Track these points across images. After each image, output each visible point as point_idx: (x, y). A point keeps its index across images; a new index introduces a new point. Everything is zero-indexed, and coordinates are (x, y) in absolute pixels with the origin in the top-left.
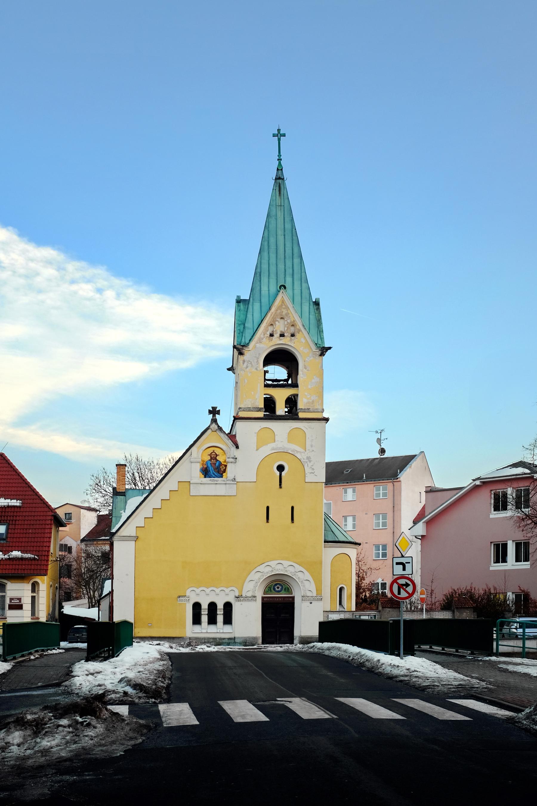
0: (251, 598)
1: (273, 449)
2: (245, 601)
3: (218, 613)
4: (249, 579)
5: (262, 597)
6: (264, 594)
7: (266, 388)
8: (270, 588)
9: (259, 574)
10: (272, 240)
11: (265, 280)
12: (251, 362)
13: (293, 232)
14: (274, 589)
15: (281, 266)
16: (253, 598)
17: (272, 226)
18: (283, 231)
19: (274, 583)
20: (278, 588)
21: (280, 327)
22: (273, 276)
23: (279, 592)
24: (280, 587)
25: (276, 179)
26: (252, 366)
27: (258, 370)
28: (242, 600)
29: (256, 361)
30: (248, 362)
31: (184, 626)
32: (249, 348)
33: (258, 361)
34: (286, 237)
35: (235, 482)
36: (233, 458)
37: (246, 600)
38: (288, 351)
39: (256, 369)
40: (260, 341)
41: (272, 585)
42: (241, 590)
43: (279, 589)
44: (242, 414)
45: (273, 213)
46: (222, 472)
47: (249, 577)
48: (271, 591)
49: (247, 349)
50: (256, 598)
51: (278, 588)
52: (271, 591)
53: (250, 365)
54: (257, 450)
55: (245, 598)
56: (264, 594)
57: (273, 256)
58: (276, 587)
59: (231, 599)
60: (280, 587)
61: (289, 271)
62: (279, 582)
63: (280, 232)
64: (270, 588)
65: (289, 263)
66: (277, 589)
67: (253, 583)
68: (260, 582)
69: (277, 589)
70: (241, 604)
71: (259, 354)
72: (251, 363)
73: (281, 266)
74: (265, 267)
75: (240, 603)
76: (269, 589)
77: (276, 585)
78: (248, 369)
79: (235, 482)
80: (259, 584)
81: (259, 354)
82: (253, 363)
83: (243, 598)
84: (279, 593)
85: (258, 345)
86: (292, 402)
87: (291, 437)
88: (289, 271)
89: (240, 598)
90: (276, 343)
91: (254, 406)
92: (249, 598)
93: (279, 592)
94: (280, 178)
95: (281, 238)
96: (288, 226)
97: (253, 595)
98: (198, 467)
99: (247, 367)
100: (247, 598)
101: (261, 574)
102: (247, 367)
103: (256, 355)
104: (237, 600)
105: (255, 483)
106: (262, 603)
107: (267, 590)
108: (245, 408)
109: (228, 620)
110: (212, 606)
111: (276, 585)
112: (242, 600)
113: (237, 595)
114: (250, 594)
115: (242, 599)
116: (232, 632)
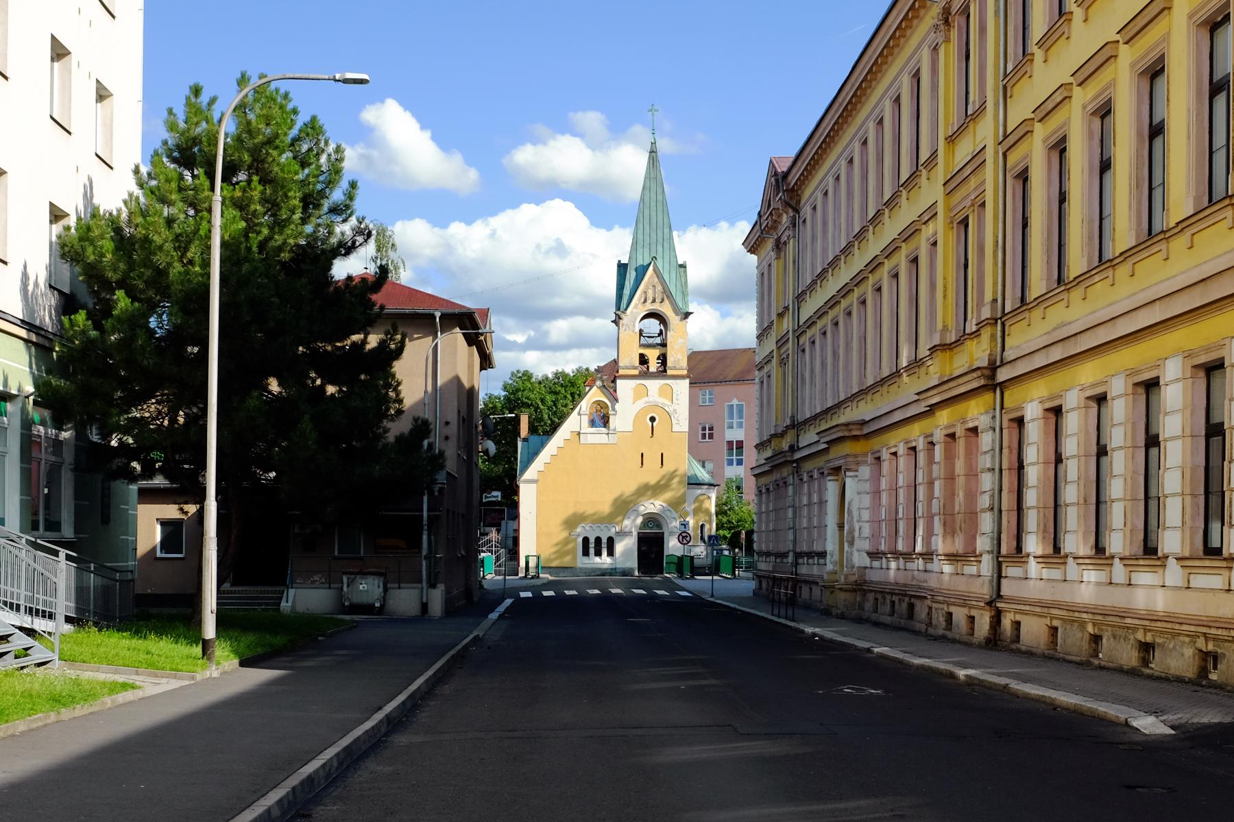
1: (646, 403)
10: (646, 212)
11: (640, 251)
17: (646, 199)
22: (647, 246)
25: (650, 152)
31: (575, 558)
33: (634, 325)
44: (621, 372)
45: (648, 185)
57: (647, 227)
61: (660, 240)
63: (653, 204)
74: (640, 237)
86: (663, 359)
87: (662, 392)
90: (650, 307)
94: (653, 152)
96: (660, 198)
98: (585, 419)
109: (611, 553)
110: (598, 540)
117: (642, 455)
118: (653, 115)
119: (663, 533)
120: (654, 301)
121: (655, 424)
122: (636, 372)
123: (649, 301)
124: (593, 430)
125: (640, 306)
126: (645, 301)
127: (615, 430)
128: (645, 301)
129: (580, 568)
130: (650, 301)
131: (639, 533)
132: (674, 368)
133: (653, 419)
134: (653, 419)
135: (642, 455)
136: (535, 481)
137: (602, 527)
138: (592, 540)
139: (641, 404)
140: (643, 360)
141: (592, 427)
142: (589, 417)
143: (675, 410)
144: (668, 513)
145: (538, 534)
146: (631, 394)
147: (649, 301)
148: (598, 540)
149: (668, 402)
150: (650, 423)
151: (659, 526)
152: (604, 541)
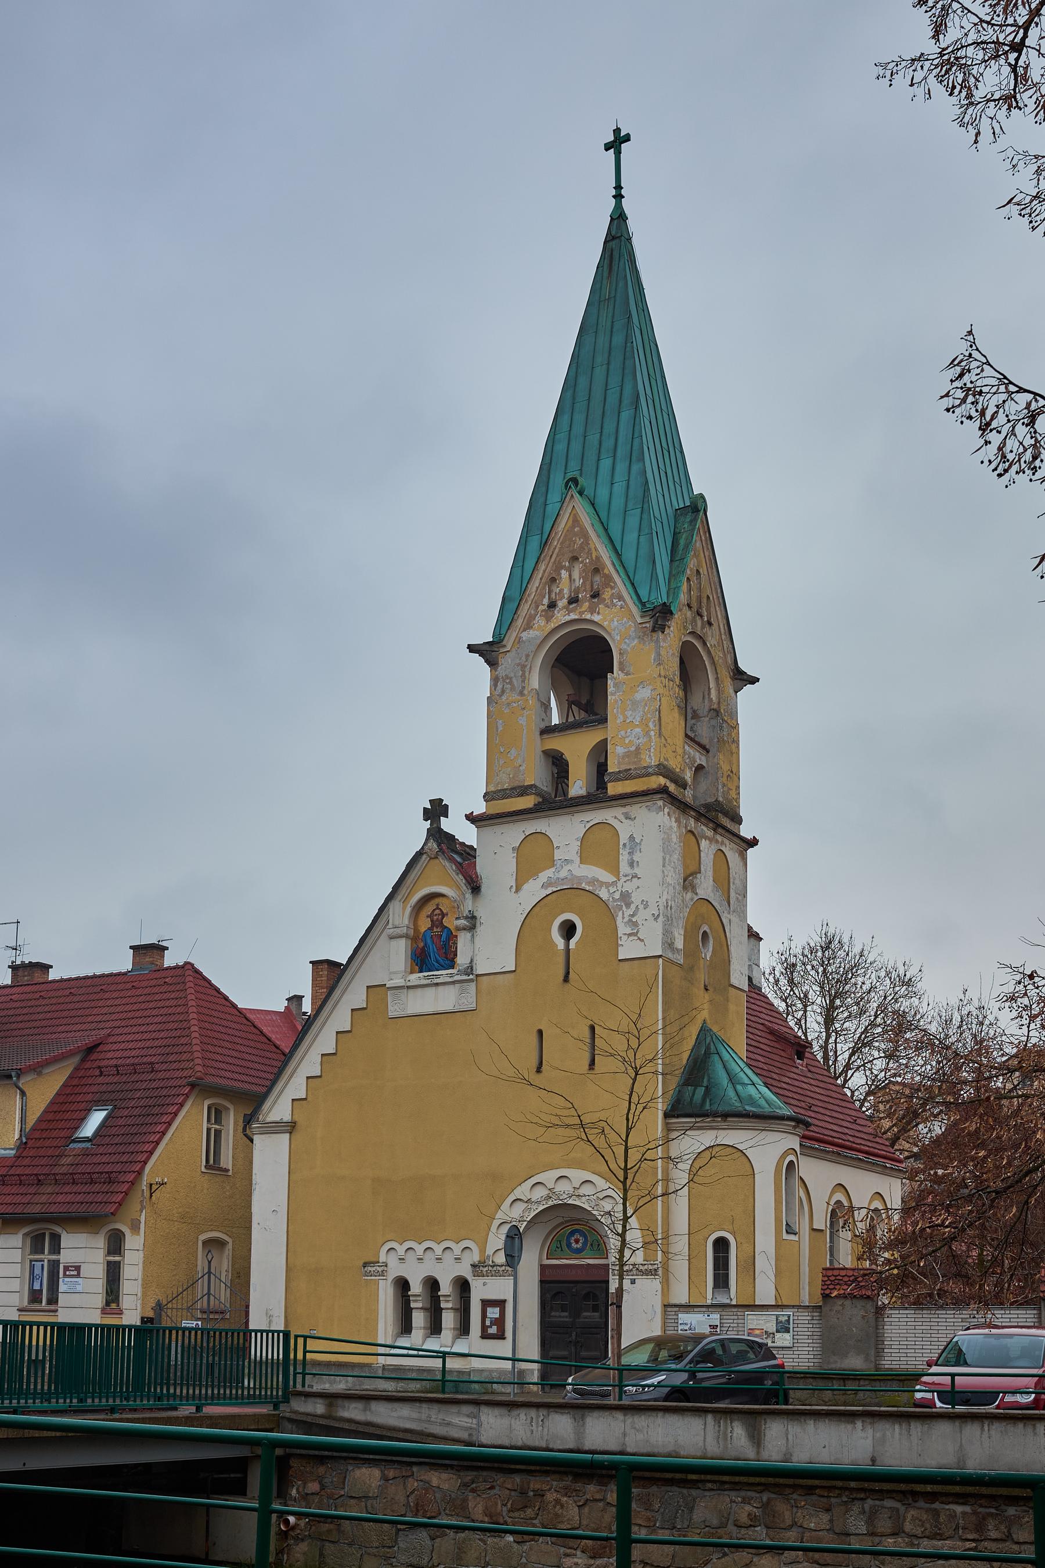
0: (503, 1268)
2: (492, 1276)
6: (547, 1259)
7: (545, 736)
9: (520, 1207)
10: (583, 382)
12: (511, 678)
13: (628, 349)
14: (569, 1245)
15: (593, 438)
18: (606, 355)
19: (569, 1230)
20: (577, 1241)
21: (567, 583)
23: (579, 1251)
26: (513, 689)
27: (524, 695)
28: (485, 1273)
29: (521, 672)
30: (504, 681)
32: (505, 646)
33: (523, 675)
34: (612, 367)
35: (471, 977)
36: (466, 918)
37: (493, 1273)
38: (581, 639)
39: (521, 693)
40: (528, 626)
43: (579, 1245)
46: (452, 956)
48: (562, 1250)
49: (502, 650)
51: (577, 1241)
52: (562, 1250)
53: (509, 686)
54: (517, 891)
55: (490, 1268)
56: (547, 1259)
57: (579, 418)
58: (572, 1241)
59: (466, 1272)
61: (608, 444)
62: (577, 1227)
65: (609, 427)
70: (484, 1284)
71: (527, 656)
72: (511, 683)
73: (593, 438)
74: (560, 447)
75: (481, 1281)
76: (559, 1246)
77: (572, 1233)
78: (504, 698)
79: (471, 977)
81: (527, 656)
82: (514, 680)
83: (486, 1269)
84: (578, 1256)
85: (525, 635)
88: (608, 444)
89: (481, 1268)
91: (516, 784)
93: (579, 1251)
95: (599, 373)
99: (503, 691)
100: (495, 1268)
101: (526, 1205)
102: (503, 691)
103: (520, 659)
104: (476, 1274)
105: (512, 975)
106: (542, 1282)
108: (494, 792)
113: (476, 1258)
117: (540, 1033)
118: (618, 154)
120: (573, 600)
121: (573, 942)
122: (527, 802)
123: (562, 603)
124: (415, 978)
125: (540, 621)
126: (552, 605)
127: (470, 970)
128: (552, 605)
130: (565, 601)
131: (543, 1268)
132: (626, 775)
133: (568, 930)
134: (568, 930)
135: (540, 1033)
136: (291, 1127)
137: (438, 1249)
138: (416, 1288)
139: (534, 890)
140: (558, 765)
141: (421, 971)
142: (414, 939)
143: (626, 897)
145: (288, 1270)
146: (508, 864)
147: (562, 603)
148: (432, 1285)
149: (605, 876)
150: (560, 943)
151: (599, 1247)
152: (446, 1288)
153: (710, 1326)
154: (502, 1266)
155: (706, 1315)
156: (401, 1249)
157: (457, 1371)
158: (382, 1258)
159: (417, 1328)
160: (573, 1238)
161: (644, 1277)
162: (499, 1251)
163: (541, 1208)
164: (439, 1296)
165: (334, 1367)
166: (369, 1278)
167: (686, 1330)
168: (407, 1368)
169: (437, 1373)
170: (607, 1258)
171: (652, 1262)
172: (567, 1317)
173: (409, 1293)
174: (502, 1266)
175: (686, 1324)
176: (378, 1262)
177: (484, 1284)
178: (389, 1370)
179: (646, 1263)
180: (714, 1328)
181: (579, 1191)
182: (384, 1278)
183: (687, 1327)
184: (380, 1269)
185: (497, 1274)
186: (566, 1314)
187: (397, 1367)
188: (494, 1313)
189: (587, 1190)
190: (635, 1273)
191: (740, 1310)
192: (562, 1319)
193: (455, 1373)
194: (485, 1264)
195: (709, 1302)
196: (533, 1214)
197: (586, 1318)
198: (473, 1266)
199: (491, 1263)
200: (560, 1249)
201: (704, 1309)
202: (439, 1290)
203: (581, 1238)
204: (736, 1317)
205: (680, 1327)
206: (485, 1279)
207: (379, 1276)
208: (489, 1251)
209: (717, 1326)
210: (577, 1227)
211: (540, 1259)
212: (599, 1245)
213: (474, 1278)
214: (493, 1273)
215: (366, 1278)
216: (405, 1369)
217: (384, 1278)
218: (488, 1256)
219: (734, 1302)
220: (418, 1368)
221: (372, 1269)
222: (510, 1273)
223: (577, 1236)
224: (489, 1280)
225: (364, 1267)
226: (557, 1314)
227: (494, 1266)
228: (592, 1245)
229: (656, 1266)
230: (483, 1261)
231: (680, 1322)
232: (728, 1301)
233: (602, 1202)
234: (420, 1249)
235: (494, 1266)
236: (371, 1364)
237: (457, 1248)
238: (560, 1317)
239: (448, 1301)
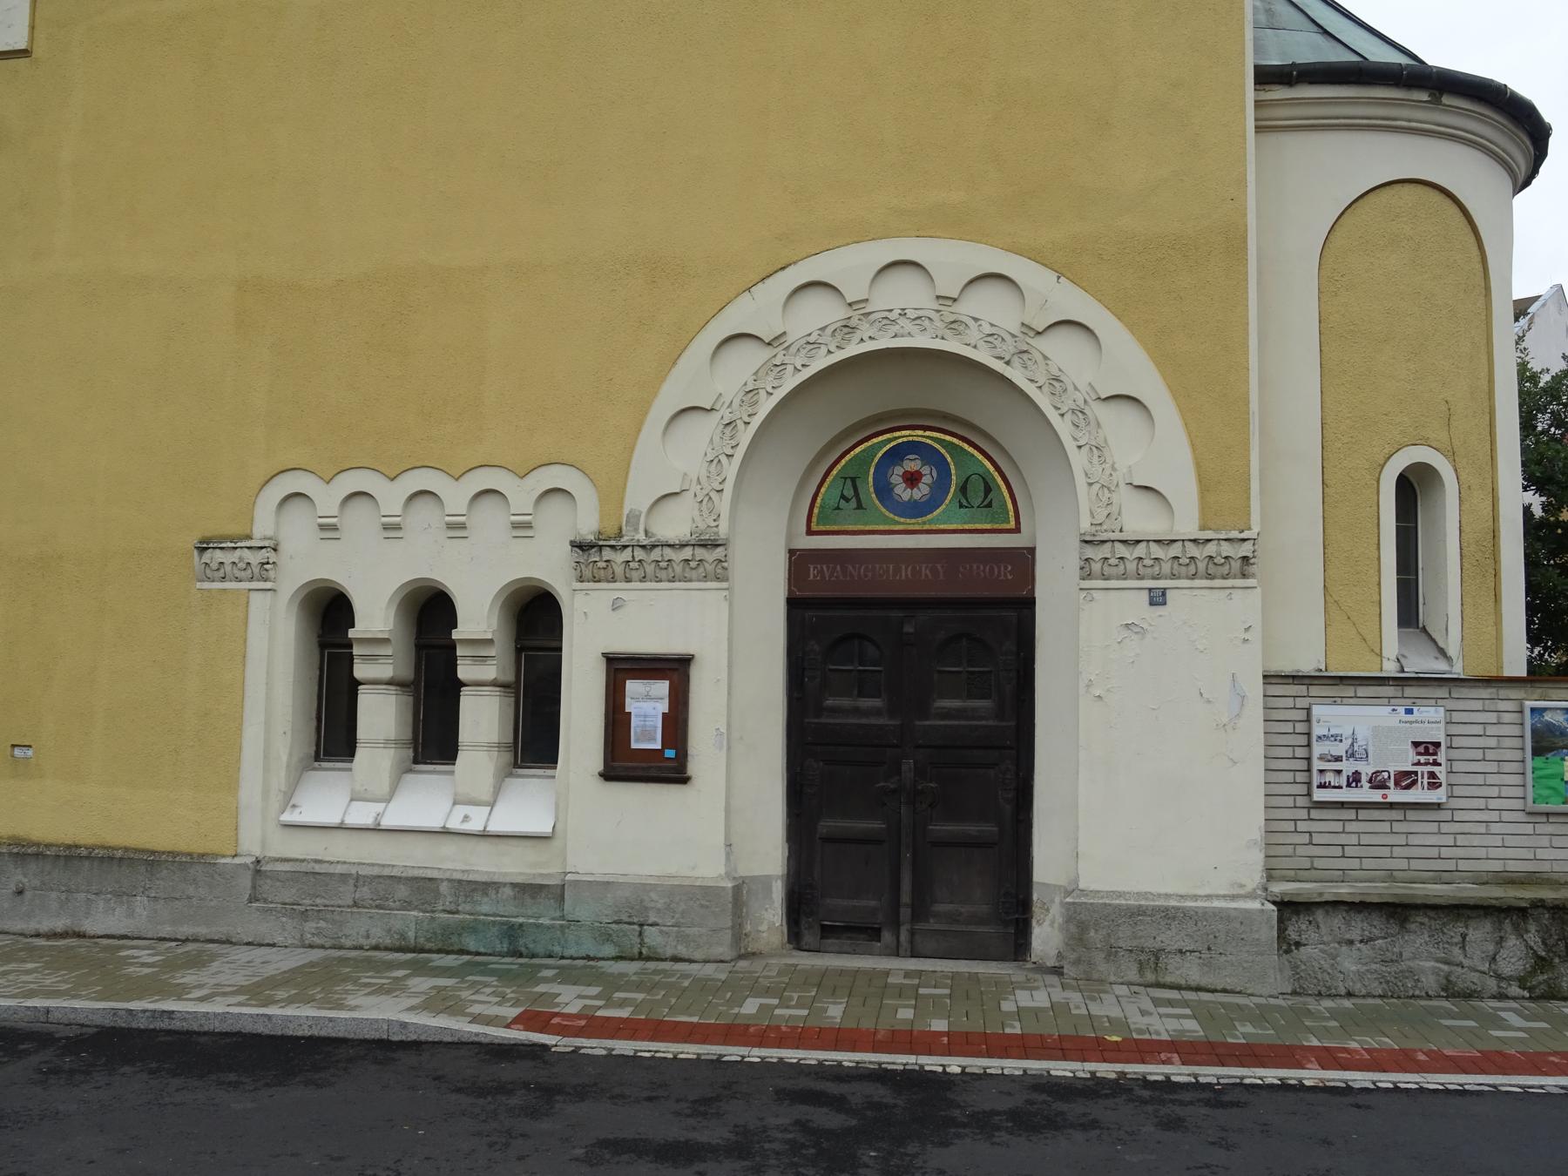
0: (687, 553)
2: (643, 579)
3: (464, 672)
4: (670, 397)
5: (792, 552)
6: (810, 532)
8: (853, 480)
9: (747, 360)
14: (884, 491)
16: (701, 553)
19: (886, 442)
20: (912, 479)
24: (929, 475)
28: (619, 570)
37: (650, 569)
41: (864, 460)
42: (612, 492)
43: (922, 491)
47: (666, 388)
48: (860, 506)
50: (719, 552)
51: (912, 479)
52: (860, 506)
55: (640, 554)
56: (810, 532)
58: (896, 476)
60: (929, 475)
64: (853, 480)
66: (903, 492)
67: (703, 431)
68: (756, 422)
69: (903, 492)
70: (616, 605)
76: (849, 492)
80: (746, 436)
83: (627, 554)
89: (607, 554)
92: (669, 553)
93: (917, 509)
97: (702, 526)
100: (657, 553)
101: (768, 352)
104: (587, 573)
106: (794, 604)
107: (833, 503)
111: (897, 454)
112: (619, 570)
113: (588, 525)
114: (675, 525)
115: (620, 558)
116: (545, 828)
119: (1024, 560)
129: (258, 869)
131: (799, 561)
137: (456, 496)
144: (1062, 351)
153: (1416, 744)
154: (683, 546)
155: (1401, 710)
156: (327, 498)
157: (514, 885)
158: (263, 525)
159: (373, 744)
160: (899, 470)
161: (1197, 583)
162: (671, 504)
163: (821, 362)
164: (452, 646)
165: (87, 863)
166: (218, 585)
167: (1338, 759)
168: (339, 869)
169: (444, 888)
170: (1017, 530)
171: (1235, 534)
172: (877, 712)
173: (352, 633)
174: (683, 546)
175: (1337, 738)
176: (249, 537)
177: (616, 605)
178: (275, 876)
179: (1209, 534)
180: (1427, 753)
181: (956, 308)
182: (268, 585)
183: (1339, 749)
184: (255, 558)
185: (663, 574)
186: (876, 703)
187: (303, 867)
188: (648, 697)
189: (991, 307)
190: (1166, 568)
191: (1503, 693)
192: (864, 721)
193: (508, 891)
194: (624, 541)
195: (1390, 669)
196: (791, 382)
197: (948, 714)
198: (581, 546)
199: (641, 536)
200: (853, 503)
201: (1388, 691)
202: (453, 624)
203: (926, 470)
204: (1492, 717)
205: (1318, 749)
206: (619, 590)
207: (252, 579)
208: (637, 498)
209: (1437, 745)
210: (905, 436)
211: (790, 536)
212: (988, 490)
213: (579, 585)
214: (650, 569)
215: (206, 585)
216: (331, 875)
217: (268, 585)
218: (633, 518)
219: (1458, 671)
220: (376, 871)
221: (227, 558)
222: (710, 568)
223: (912, 464)
224: (632, 593)
225: (202, 550)
226: (845, 702)
227: (654, 546)
228: (963, 489)
229: (1248, 546)
230: (611, 530)
231: (1318, 730)
232: (1438, 667)
233: (1042, 344)
234: (392, 496)
235: (654, 546)
236: (216, 856)
237: (521, 494)
238: (856, 711)
239: (483, 659)
